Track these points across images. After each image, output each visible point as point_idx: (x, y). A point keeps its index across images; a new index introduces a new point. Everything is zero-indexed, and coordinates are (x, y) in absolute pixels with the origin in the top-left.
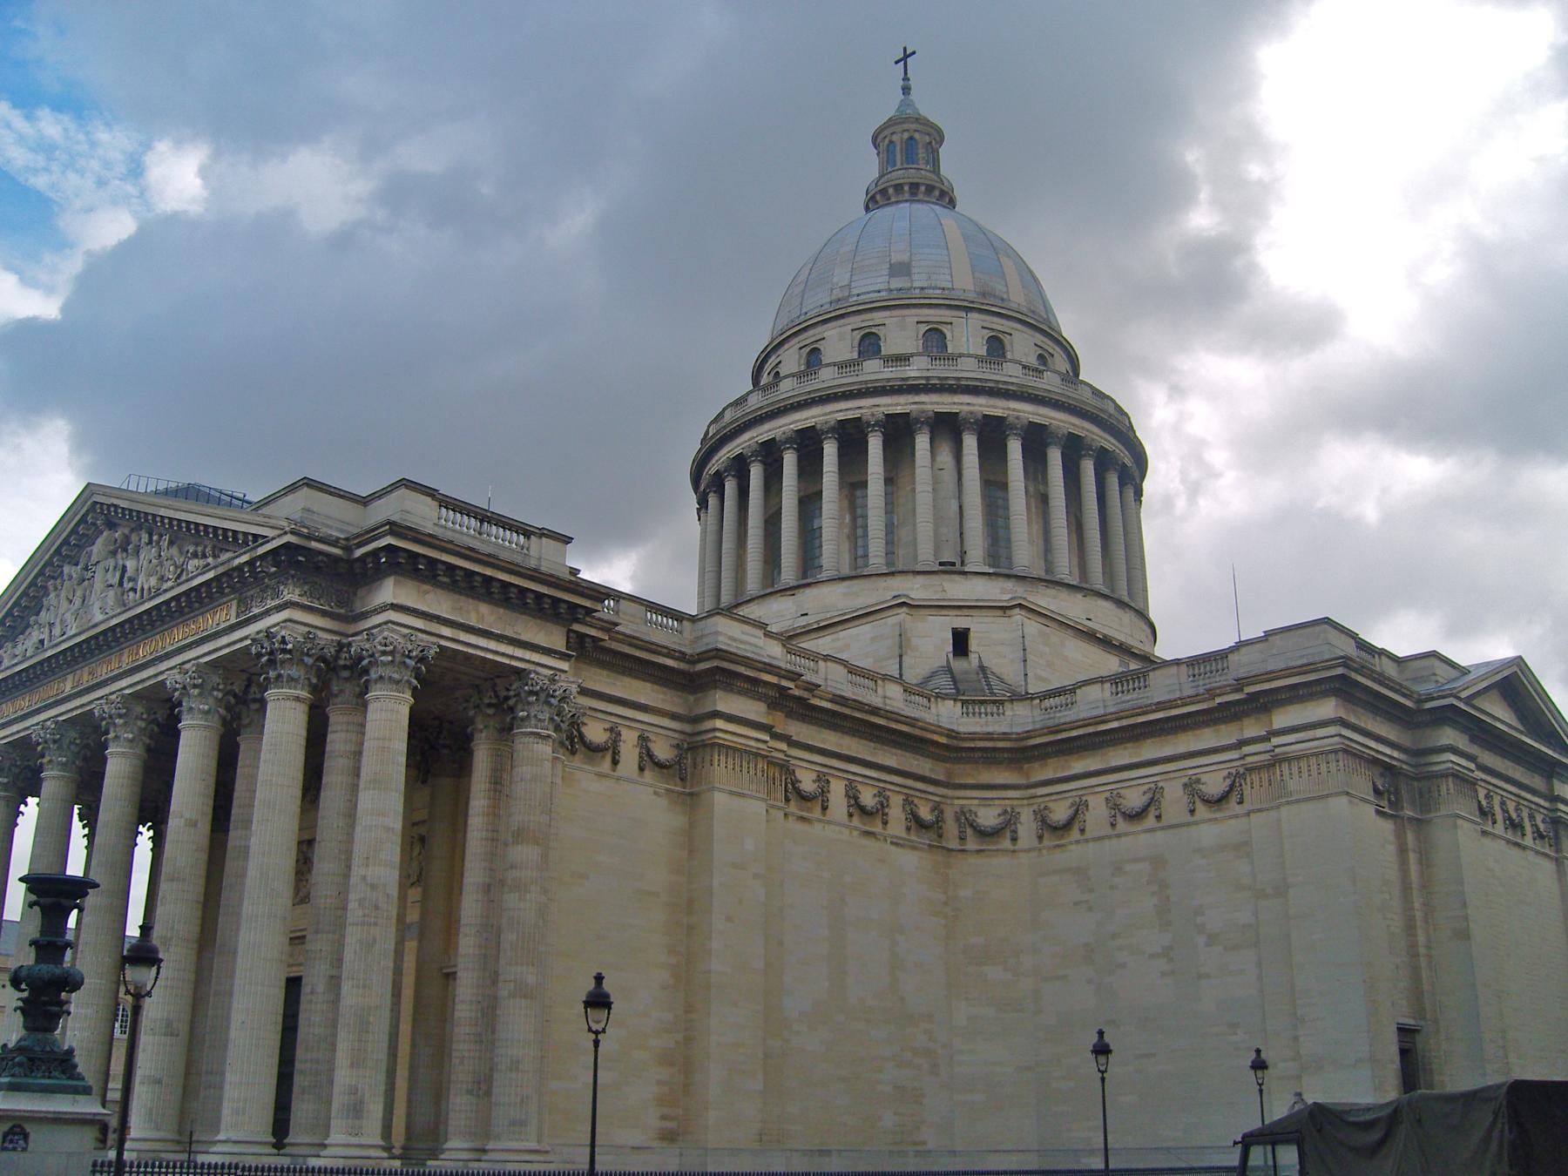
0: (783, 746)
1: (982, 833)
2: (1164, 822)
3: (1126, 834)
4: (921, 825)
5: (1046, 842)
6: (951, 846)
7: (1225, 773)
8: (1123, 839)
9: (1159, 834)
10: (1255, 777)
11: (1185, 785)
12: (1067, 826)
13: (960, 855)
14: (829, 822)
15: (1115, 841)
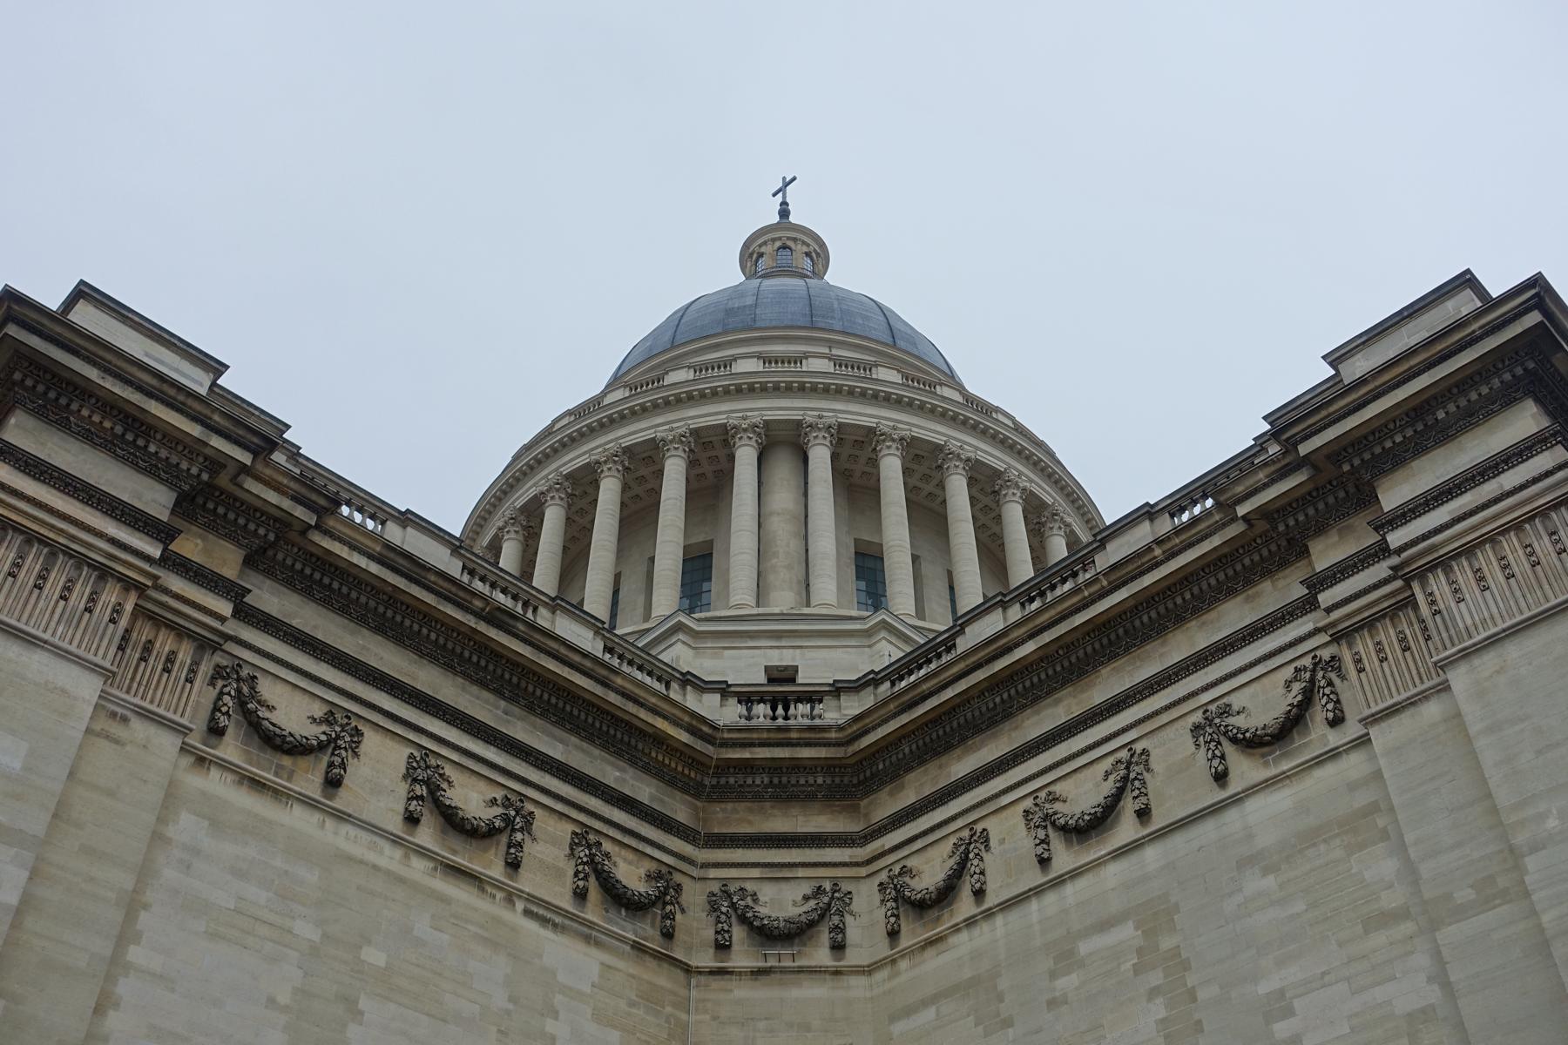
0: (225, 608)
1: (767, 935)
2: (1158, 822)
3: (1074, 874)
4: (617, 896)
5: (905, 941)
6: (694, 962)
7: (1288, 672)
8: (1069, 889)
9: (1151, 854)
10: (1364, 645)
11: (1197, 729)
12: (946, 894)
13: (716, 983)
14: (342, 817)
15: (1051, 898)
